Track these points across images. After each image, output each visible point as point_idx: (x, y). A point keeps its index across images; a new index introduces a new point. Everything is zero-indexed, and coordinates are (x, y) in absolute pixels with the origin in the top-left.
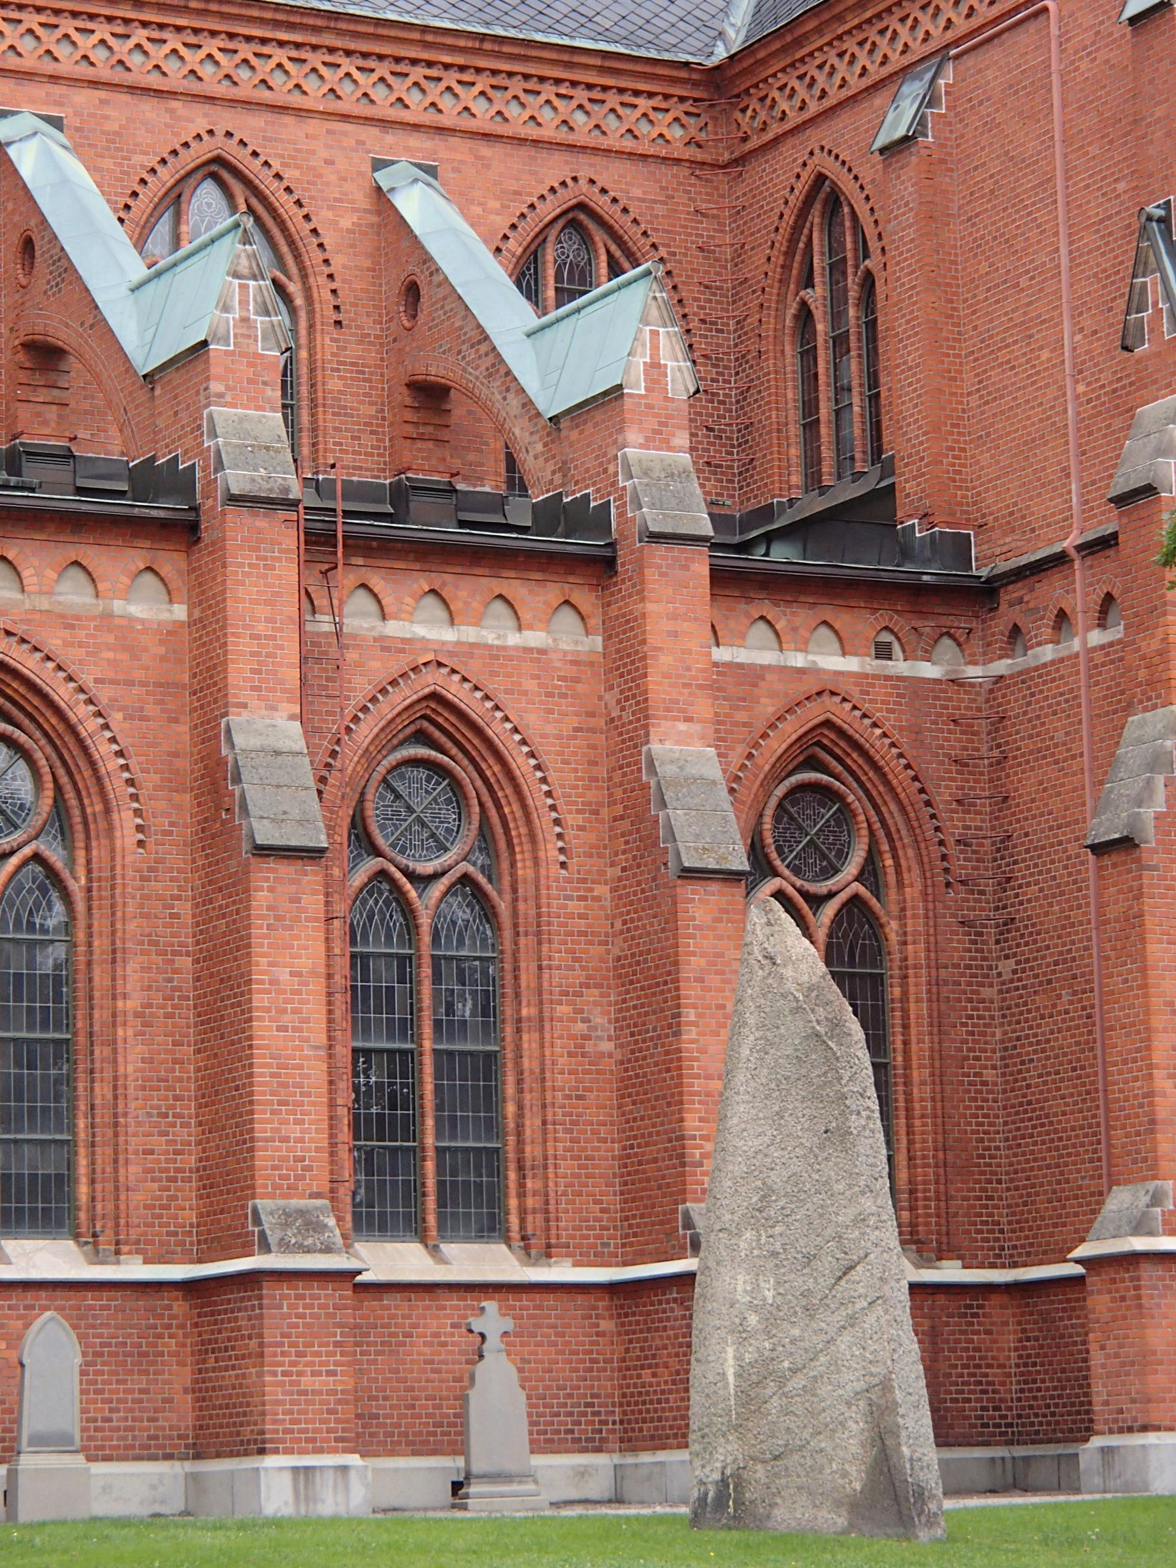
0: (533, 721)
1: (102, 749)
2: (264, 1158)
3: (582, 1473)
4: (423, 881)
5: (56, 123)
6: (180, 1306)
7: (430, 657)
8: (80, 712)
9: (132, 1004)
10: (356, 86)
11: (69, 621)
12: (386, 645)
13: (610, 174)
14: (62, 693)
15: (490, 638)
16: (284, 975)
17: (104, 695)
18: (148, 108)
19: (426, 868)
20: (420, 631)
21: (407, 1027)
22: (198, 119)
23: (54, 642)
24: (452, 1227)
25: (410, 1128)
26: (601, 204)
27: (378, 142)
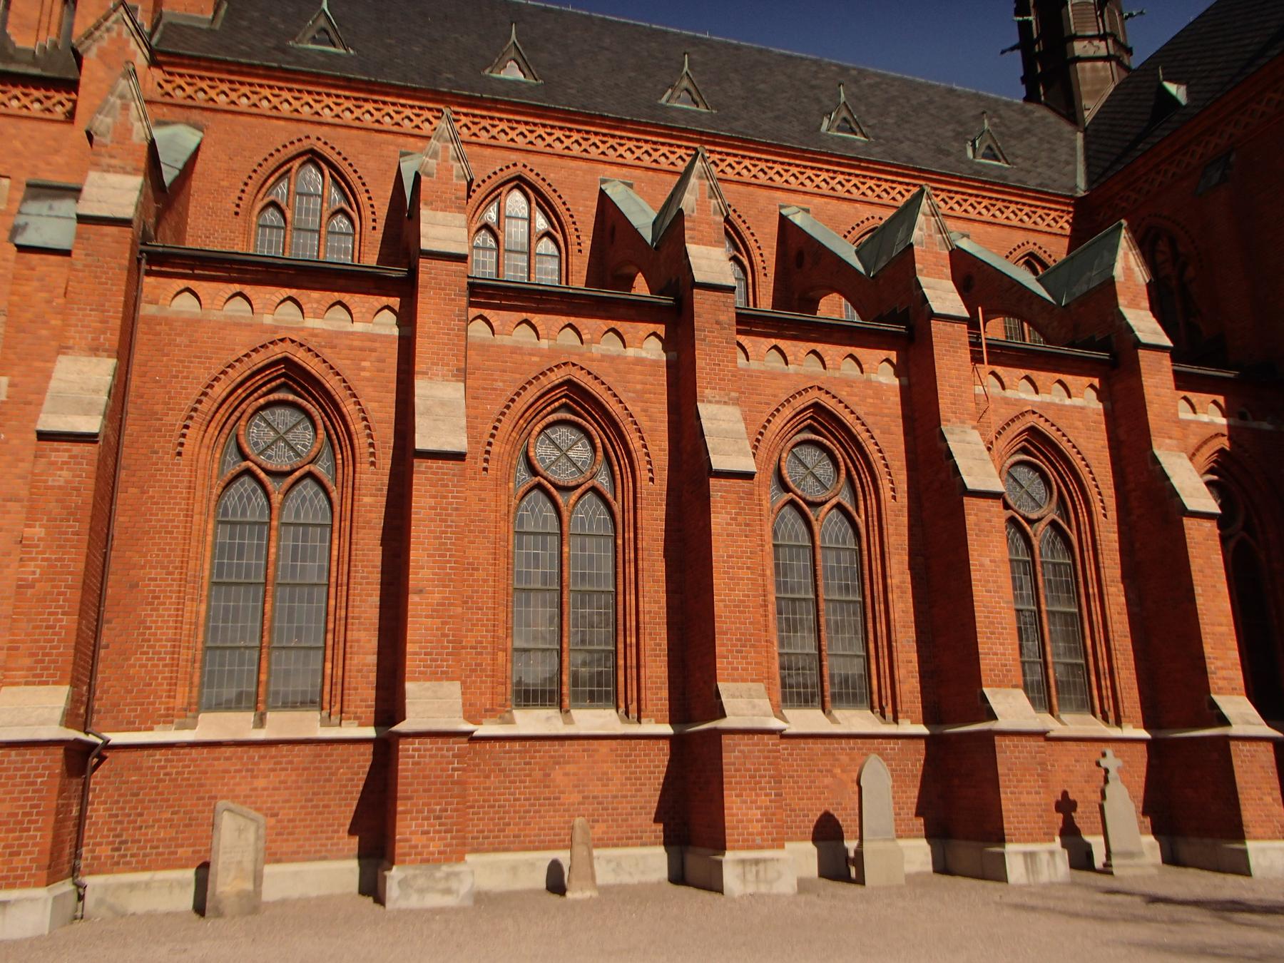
0: (1082, 443)
2: (985, 664)
7: (1029, 408)
11: (849, 383)
12: (1006, 401)
13: (1042, 240)
14: (848, 419)
15: (1057, 401)
16: (987, 561)
17: (869, 421)
18: (845, 206)
19: (1034, 516)
20: (1023, 396)
23: (843, 394)
24: (1066, 705)
26: (1040, 254)
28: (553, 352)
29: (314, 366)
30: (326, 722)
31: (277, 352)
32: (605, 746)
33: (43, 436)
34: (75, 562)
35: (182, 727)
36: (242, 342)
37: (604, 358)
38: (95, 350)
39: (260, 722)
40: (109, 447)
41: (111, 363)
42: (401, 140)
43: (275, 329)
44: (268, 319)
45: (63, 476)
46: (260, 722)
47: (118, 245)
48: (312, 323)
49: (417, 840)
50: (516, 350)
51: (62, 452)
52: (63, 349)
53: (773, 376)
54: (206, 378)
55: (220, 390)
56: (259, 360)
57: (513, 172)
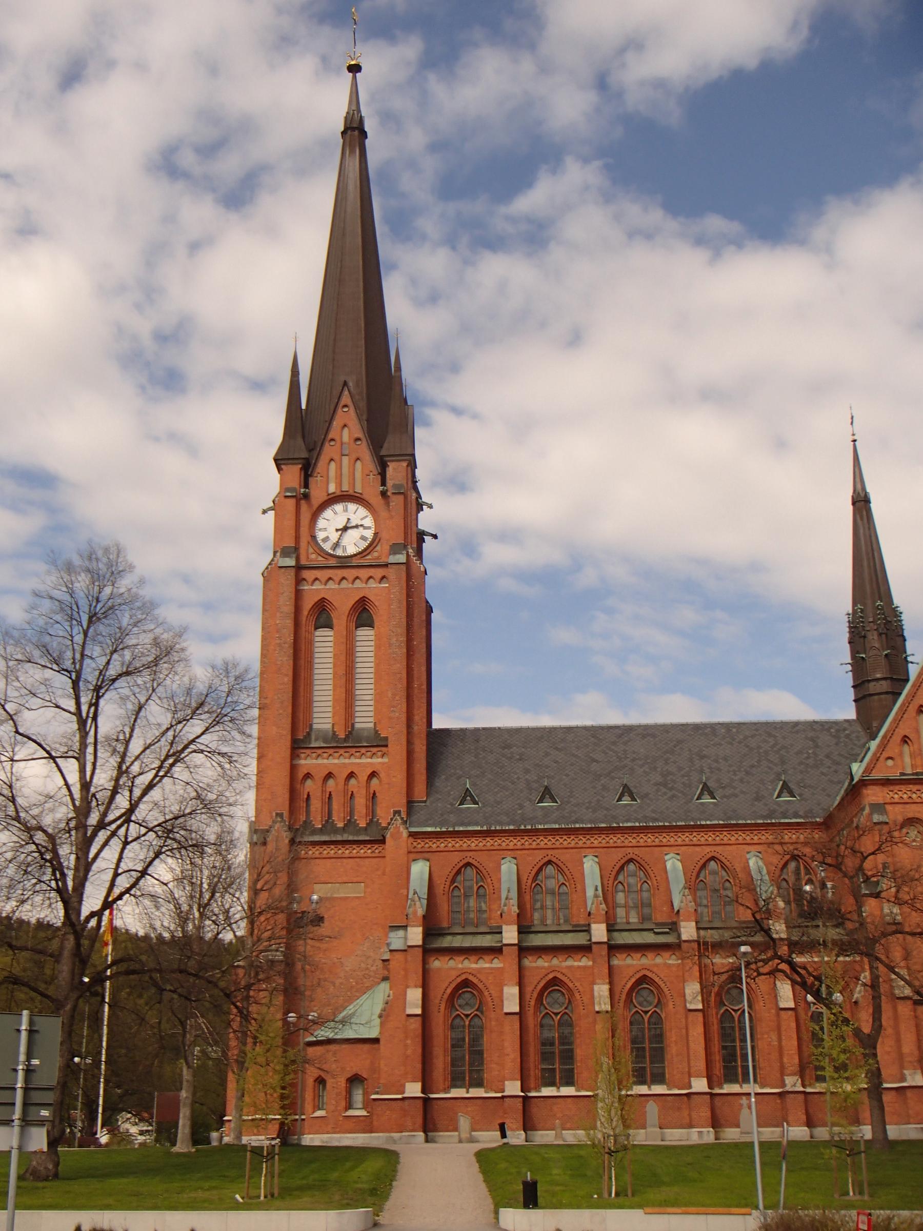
1: (665, 990)
3: (773, 1132)
4: (735, 1011)
5: (678, 854)
6: (685, 1098)
8: (660, 983)
9: (674, 1039)
10: (741, 836)
11: (657, 965)
14: (657, 980)
17: (665, 979)
18: (698, 849)
19: (736, 1008)
21: (734, 1041)
22: (708, 849)
23: (655, 970)
25: (736, 1061)
27: (747, 848)
28: (549, 967)
29: (475, 980)
30: (486, 1092)
31: (463, 977)
32: (569, 1100)
33: (408, 1016)
34: (420, 1051)
35: (446, 1093)
36: (454, 974)
37: (568, 967)
38: (416, 987)
39: (468, 1092)
40: (425, 1016)
41: (420, 990)
42: (501, 852)
43: (463, 969)
44: (460, 966)
45: (413, 1026)
46: (468, 1092)
47: (419, 952)
48: (474, 966)
49: (511, 1125)
50: (537, 968)
51: (412, 1020)
52: (407, 987)
53: (629, 966)
54: (444, 987)
55: (449, 991)
56: (459, 980)
57: (546, 859)
